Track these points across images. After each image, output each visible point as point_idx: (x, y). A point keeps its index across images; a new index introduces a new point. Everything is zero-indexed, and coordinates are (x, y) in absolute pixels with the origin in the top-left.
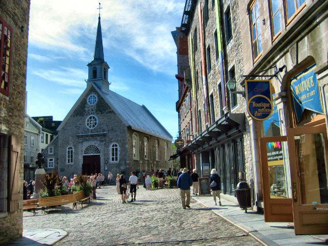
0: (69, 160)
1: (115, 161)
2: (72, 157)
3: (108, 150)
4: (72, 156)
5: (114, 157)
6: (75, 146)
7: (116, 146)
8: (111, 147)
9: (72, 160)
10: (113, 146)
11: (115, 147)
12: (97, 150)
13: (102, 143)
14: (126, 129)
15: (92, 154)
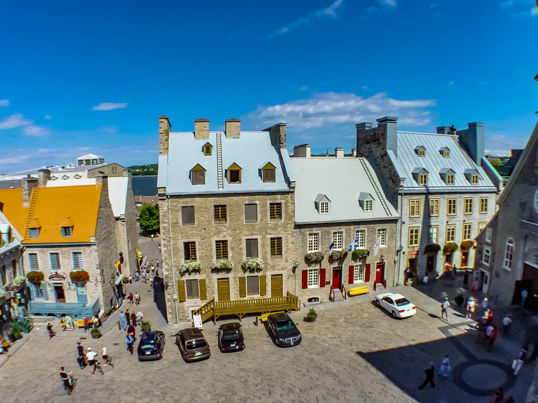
2: (511, 259)
9: (510, 263)
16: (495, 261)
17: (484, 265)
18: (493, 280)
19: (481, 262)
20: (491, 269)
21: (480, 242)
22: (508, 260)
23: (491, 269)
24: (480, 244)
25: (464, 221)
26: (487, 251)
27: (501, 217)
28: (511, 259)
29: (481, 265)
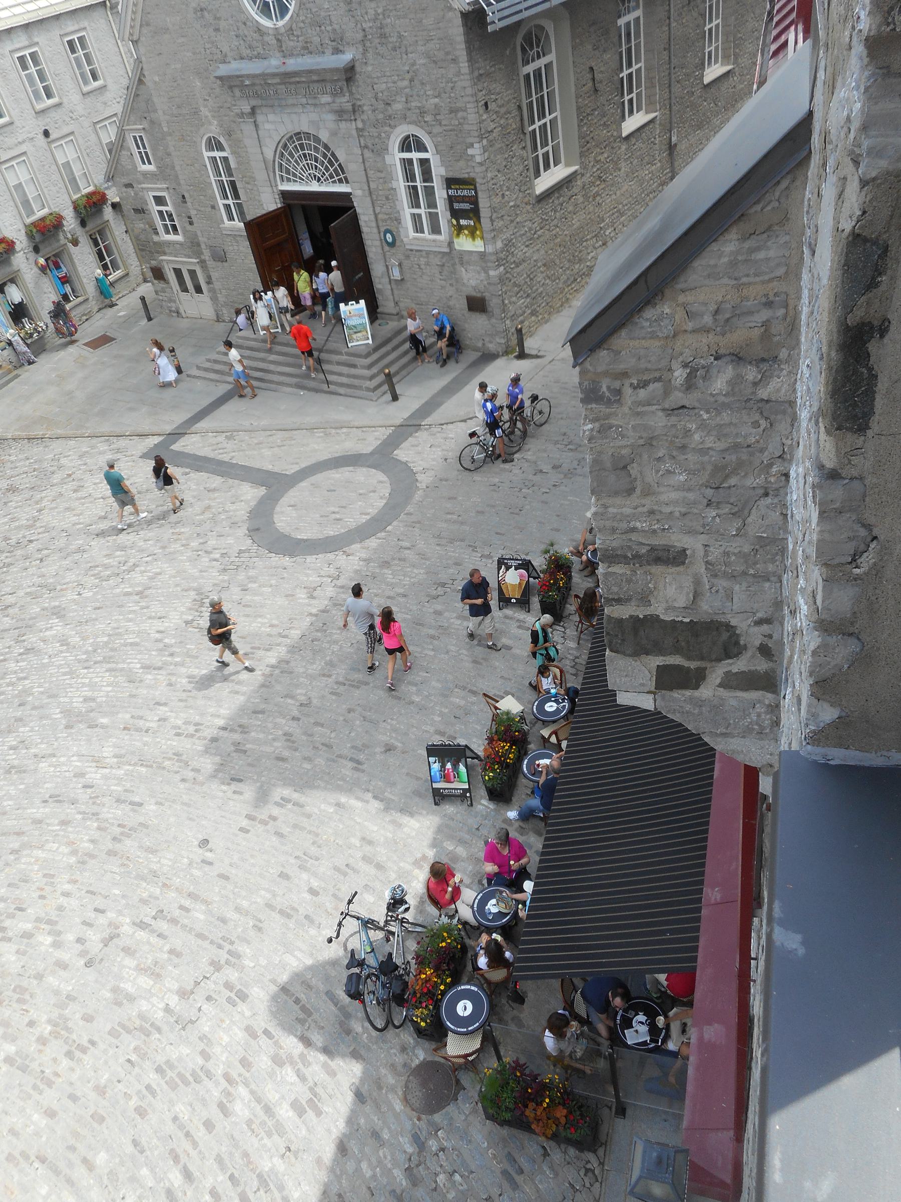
0: (227, 207)
1: (427, 235)
2: (236, 196)
3: (387, 176)
4: (233, 184)
5: (422, 211)
6: (229, 134)
7: (421, 148)
8: (396, 157)
9: (239, 206)
10: (407, 145)
11: (415, 156)
12: (340, 173)
13: (343, 125)
14: (457, 30)
15: (315, 187)
16: (194, 220)
17: (169, 243)
18: (215, 275)
19: (156, 238)
20: (194, 246)
21: (125, 180)
22: (230, 202)
23: (194, 246)
24: (129, 185)
25: (46, 134)
26: (159, 201)
27: (151, 78)
28: (236, 196)
29: (161, 248)
